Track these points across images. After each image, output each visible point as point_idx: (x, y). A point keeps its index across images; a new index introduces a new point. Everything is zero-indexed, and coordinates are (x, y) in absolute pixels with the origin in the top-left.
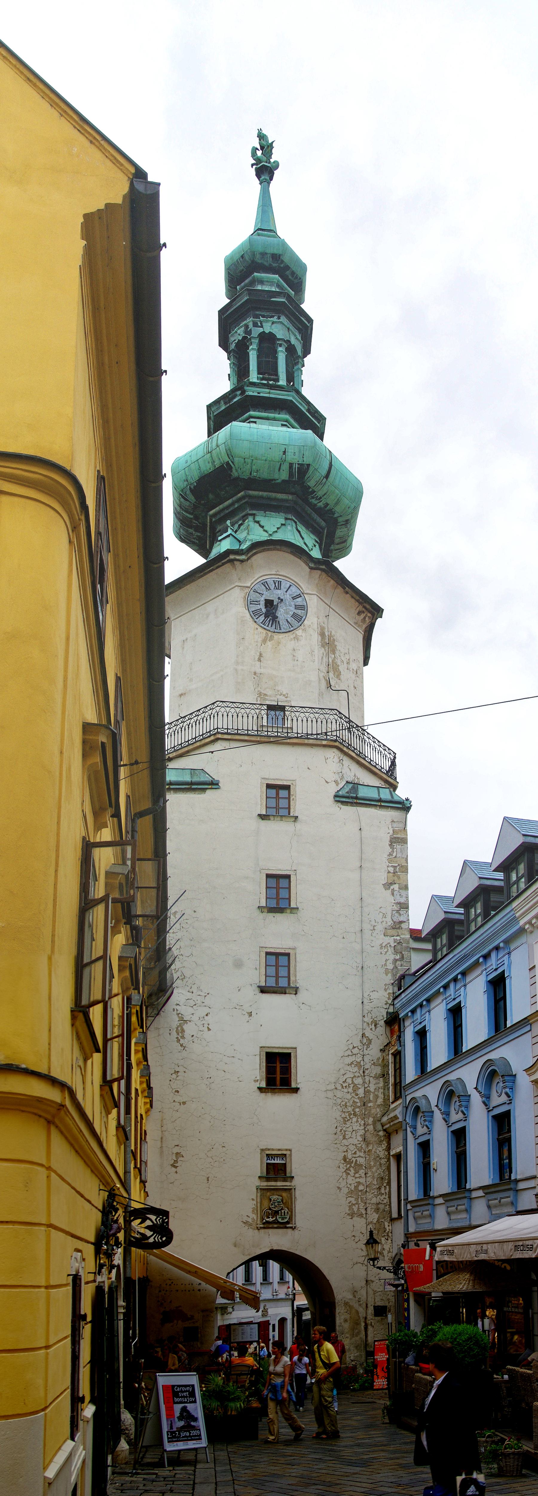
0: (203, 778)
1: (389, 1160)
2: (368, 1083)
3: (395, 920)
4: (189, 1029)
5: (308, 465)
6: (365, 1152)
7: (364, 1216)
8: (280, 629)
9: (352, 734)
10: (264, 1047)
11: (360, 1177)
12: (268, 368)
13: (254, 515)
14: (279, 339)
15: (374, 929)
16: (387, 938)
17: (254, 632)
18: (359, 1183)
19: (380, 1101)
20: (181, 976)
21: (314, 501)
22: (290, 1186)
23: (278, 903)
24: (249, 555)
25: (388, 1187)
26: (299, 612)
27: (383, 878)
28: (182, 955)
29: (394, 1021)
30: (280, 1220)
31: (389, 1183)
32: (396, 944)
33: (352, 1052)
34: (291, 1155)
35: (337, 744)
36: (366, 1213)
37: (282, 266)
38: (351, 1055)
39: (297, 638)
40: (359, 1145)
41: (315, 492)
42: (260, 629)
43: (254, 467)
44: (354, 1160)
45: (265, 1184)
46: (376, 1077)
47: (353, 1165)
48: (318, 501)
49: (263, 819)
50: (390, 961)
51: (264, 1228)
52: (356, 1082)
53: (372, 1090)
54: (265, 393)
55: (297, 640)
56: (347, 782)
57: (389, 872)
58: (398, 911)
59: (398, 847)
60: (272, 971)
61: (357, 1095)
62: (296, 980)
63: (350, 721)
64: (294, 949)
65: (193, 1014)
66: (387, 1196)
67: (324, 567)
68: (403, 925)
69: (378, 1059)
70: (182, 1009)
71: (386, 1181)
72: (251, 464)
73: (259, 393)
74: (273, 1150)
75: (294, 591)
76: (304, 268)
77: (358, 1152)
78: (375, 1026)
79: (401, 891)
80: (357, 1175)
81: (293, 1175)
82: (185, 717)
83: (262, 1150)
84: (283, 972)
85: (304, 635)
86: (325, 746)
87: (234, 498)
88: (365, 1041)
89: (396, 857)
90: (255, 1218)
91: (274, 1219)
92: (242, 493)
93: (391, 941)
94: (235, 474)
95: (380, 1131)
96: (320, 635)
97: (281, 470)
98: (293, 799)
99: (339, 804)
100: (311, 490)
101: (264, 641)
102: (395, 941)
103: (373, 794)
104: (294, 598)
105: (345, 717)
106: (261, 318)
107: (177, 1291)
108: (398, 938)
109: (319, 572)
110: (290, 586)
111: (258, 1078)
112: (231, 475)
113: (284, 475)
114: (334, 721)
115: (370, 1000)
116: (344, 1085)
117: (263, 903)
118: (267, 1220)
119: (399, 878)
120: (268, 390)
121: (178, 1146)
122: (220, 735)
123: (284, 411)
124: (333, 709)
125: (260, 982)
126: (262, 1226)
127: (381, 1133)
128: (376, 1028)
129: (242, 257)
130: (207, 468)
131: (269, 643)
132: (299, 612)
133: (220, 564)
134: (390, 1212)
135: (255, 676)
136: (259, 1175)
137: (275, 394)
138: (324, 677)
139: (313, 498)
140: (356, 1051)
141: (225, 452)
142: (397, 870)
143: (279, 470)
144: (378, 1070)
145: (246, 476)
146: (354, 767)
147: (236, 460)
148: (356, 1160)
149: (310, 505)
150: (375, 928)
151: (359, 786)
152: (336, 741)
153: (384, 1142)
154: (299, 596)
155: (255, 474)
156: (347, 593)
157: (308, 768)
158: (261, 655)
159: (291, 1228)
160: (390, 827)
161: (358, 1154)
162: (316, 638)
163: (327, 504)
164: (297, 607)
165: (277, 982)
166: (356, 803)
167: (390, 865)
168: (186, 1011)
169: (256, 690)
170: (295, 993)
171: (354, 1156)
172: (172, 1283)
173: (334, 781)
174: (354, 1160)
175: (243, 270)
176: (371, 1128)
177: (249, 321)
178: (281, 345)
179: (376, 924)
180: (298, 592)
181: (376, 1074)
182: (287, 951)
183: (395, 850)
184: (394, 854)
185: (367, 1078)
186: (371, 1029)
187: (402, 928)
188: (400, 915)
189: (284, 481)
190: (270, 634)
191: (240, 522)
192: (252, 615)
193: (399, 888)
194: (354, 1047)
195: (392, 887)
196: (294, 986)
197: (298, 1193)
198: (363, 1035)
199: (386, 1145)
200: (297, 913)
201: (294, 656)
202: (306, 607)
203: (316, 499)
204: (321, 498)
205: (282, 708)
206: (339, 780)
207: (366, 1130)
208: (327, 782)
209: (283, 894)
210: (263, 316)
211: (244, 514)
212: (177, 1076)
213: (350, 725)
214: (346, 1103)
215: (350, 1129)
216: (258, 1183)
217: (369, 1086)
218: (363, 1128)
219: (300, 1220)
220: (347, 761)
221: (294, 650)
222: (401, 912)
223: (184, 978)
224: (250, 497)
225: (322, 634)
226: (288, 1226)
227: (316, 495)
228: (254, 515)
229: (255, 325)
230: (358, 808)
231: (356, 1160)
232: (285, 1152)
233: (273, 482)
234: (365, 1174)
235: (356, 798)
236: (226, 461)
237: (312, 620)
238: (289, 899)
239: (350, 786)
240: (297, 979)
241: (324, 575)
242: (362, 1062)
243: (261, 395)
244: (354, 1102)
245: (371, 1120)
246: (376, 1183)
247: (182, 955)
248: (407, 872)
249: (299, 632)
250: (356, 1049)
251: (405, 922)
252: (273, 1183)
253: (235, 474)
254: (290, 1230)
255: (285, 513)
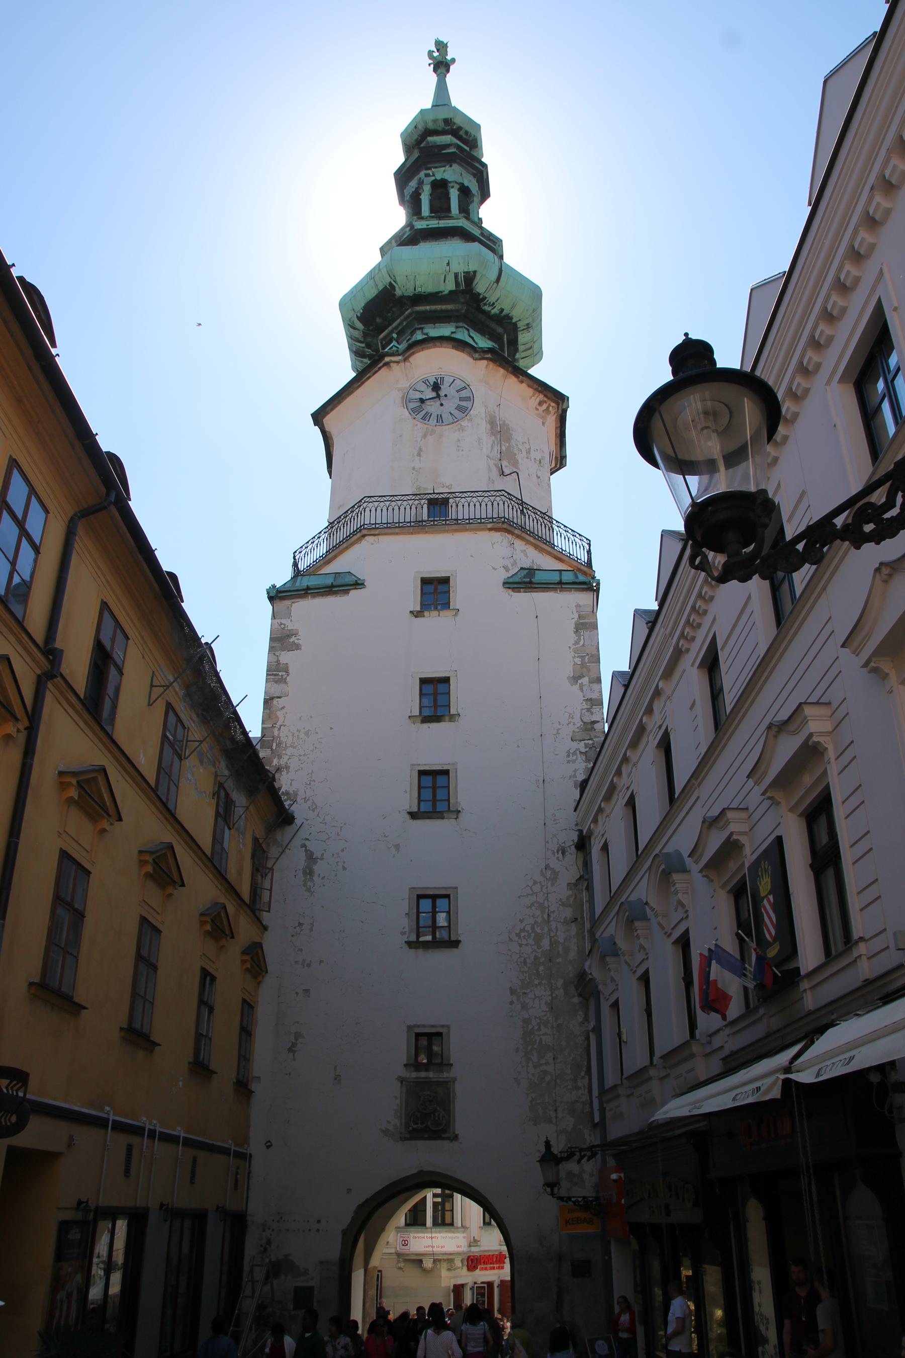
0: (349, 580)
1: (588, 1038)
2: (555, 931)
3: (585, 720)
4: (318, 868)
5: (475, 272)
6: (552, 1027)
7: (554, 1121)
8: (442, 422)
9: (527, 516)
10: (414, 888)
11: (547, 1063)
12: (440, 207)
13: (422, 329)
14: (450, 182)
15: (558, 733)
16: (575, 743)
17: (412, 428)
18: (545, 1072)
19: (572, 955)
20: (312, 806)
21: (487, 308)
22: (448, 1078)
23: (435, 711)
24: (406, 355)
25: (587, 1077)
26: (464, 404)
27: (569, 671)
28: (314, 781)
29: (582, 844)
30: (433, 1128)
31: (589, 1072)
32: (587, 749)
33: (532, 891)
34: (448, 1033)
35: (505, 526)
36: (556, 1117)
37: (455, 127)
38: (532, 895)
39: (462, 429)
40: (545, 1018)
41: (486, 298)
42: (420, 425)
43: (418, 283)
44: (538, 1038)
45: (414, 1075)
46: (566, 922)
47: (535, 1046)
48: (491, 308)
49: (416, 617)
50: (581, 771)
51: (411, 1139)
52: (538, 930)
53: (561, 940)
54: (434, 224)
55: (462, 430)
56: (522, 569)
57: (575, 664)
58: (588, 710)
59: (587, 634)
60: (427, 794)
61: (539, 947)
62: (457, 802)
63: (522, 503)
64: (455, 764)
65: (325, 850)
66: (586, 1090)
67: (489, 356)
68: (596, 726)
69: (568, 898)
70: (311, 846)
71: (585, 1069)
72: (415, 280)
73: (428, 225)
74: (424, 1026)
75: (459, 384)
76: (478, 127)
77: (542, 1027)
78: (563, 853)
79: (591, 685)
80: (543, 1061)
81: (451, 1062)
82: (333, 522)
83: (410, 1028)
84: (440, 794)
85: (470, 424)
86: (490, 529)
87: (402, 318)
88: (549, 873)
89: (583, 645)
90: (398, 1124)
91: (424, 1126)
92: (409, 311)
93: (581, 746)
94: (398, 293)
95: (574, 996)
96: (489, 423)
97: (447, 281)
98: (453, 592)
99: (510, 591)
100: (481, 296)
101: (425, 436)
102: (586, 746)
103: (555, 578)
104: (458, 391)
105: (517, 498)
106: (433, 170)
107: (288, 1230)
108: (590, 742)
109: (485, 362)
110: (454, 380)
111: (407, 929)
112: (395, 295)
113: (450, 286)
114: (501, 503)
115: (555, 820)
116: (522, 934)
117: (416, 712)
118: (415, 1126)
119: (589, 670)
120: (437, 222)
121: (298, 1022)
122: (366, 531)
123: (455, 238)
124: (500, 491)
125: (410, 807)
126: (407, 1136)
127: (576, 1000)
128: (563, 857)
129: (416, 127)
130: (371, 293)
131: (430, 439)
132: (464, 404)
133: (376, 369)
134: (591, 1114)
135: (414, 472)
136: (405, 1062)
137: (444, 223)
138: (496, 465)
139: (485, 304)
140: (537, 888)
141: (386, 272)
142: (586, 660)
143: (444, 282)
144: (568, 913)
145: (410, 293)
146: (531, 551)
147: (398, 279)
148: (541, 1040)
149: (484, 312)
150: (560, 731)
151: (536, 572)
152: (504, 522)
153: (580, 1013)
154: (465, 388)
155: (420, 289)
156: (522, 382)
157: (472, 556)
158: (420, 449)
159: (448, 1138)
160: (575, 611)
161: (543, 1030)
162: (483, 427)
163: (502, 310)
164: (461, 399)
165: (434, 805)
166: (531, 587)
167: (576, 655)
168: (315, 847)
169: (415, 485)
170: (456, 817)
171: (537, 1033)
172: (281, 1218)
173: (503, 567)
174: (538, 1038)
175: (417, 139)
176: (561, 992)
177: (422, 174)
178: (452, 187)
179: (560, 727)
180: (463, 385)
181: (566, 917)
182: (445, 768)
183: (582, 637)
184: (582, 643)
185: (553, 925)
186: (558, 858)
187: (595, 730)
188: (592, 714)
189: (451, 292)
190: (430, 428)
191: (408, 338)
192: (411, 412)
193: (590, 682)
194: (535, 883)
195: (580, 681)
196: (455, 809)
197: (459, 1089)
198: (547, 867)
199: (583, 1016)
200: (458, 721)
201: (458, 446)
202: (472, 398)
203: (489, 306)
204: (494, 304)
205: (445, 502)
206: (510, 566)
207: (554, 995)
208: (494, 569)
209: (441, 700)
210: (436, 167)
211: (412, 330)
212: (302, 930)
213: (523, 507)
214: (525, 960)
215: (531, 995)
216: (403, 1073)
217: (556, 935)
218: (549, 993)
219: (461, 1125)
220: (519, 544)
221: (459, 440)
222: (594, 710)
223: (316, 808)
224: (418, 312)
225: (492, 422)
226: (443, 1136)
227: (488, 301)
228: (422, 329)
229: (427, 175)
230: (533, 594)
231: (541, 1040)
232: (440, 1030)
233: (440, 294)
234: (554, 1059)
235: (531, 582)
236: (388, 282)
237: (478, 409)
238: (449, 706)
239: (525, 572)
240: (459, 800)
241: (491, 365)
242: (546, 902)
243: (430, 226)
244: (536, 958)
245: (560, 982)
246: (569, 1072)
247: (314, 781)
248: (600, 663)
249: (464, 423)
250: (538, 885)
251: (599, 722)
252: (423, 1074)
253: (398, 293)
254: (446, 1143)
255: (456, 322)
